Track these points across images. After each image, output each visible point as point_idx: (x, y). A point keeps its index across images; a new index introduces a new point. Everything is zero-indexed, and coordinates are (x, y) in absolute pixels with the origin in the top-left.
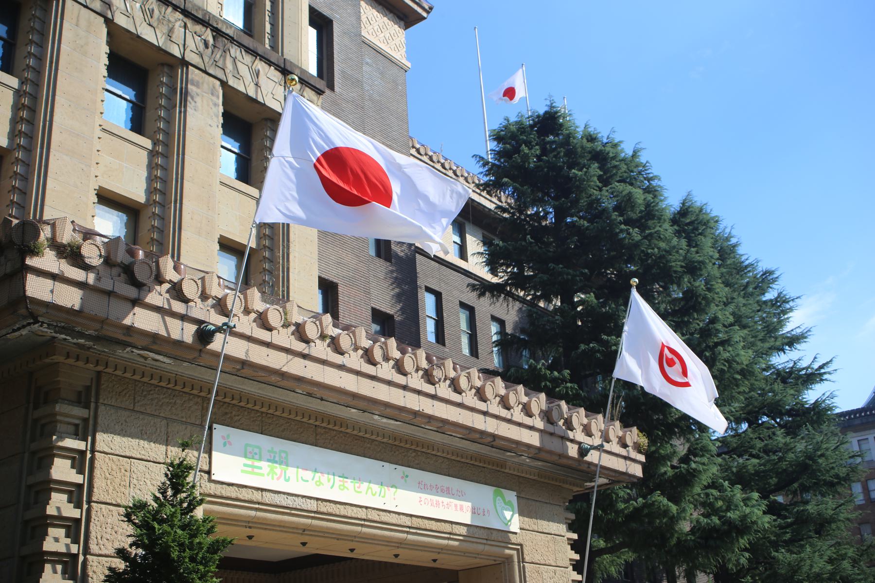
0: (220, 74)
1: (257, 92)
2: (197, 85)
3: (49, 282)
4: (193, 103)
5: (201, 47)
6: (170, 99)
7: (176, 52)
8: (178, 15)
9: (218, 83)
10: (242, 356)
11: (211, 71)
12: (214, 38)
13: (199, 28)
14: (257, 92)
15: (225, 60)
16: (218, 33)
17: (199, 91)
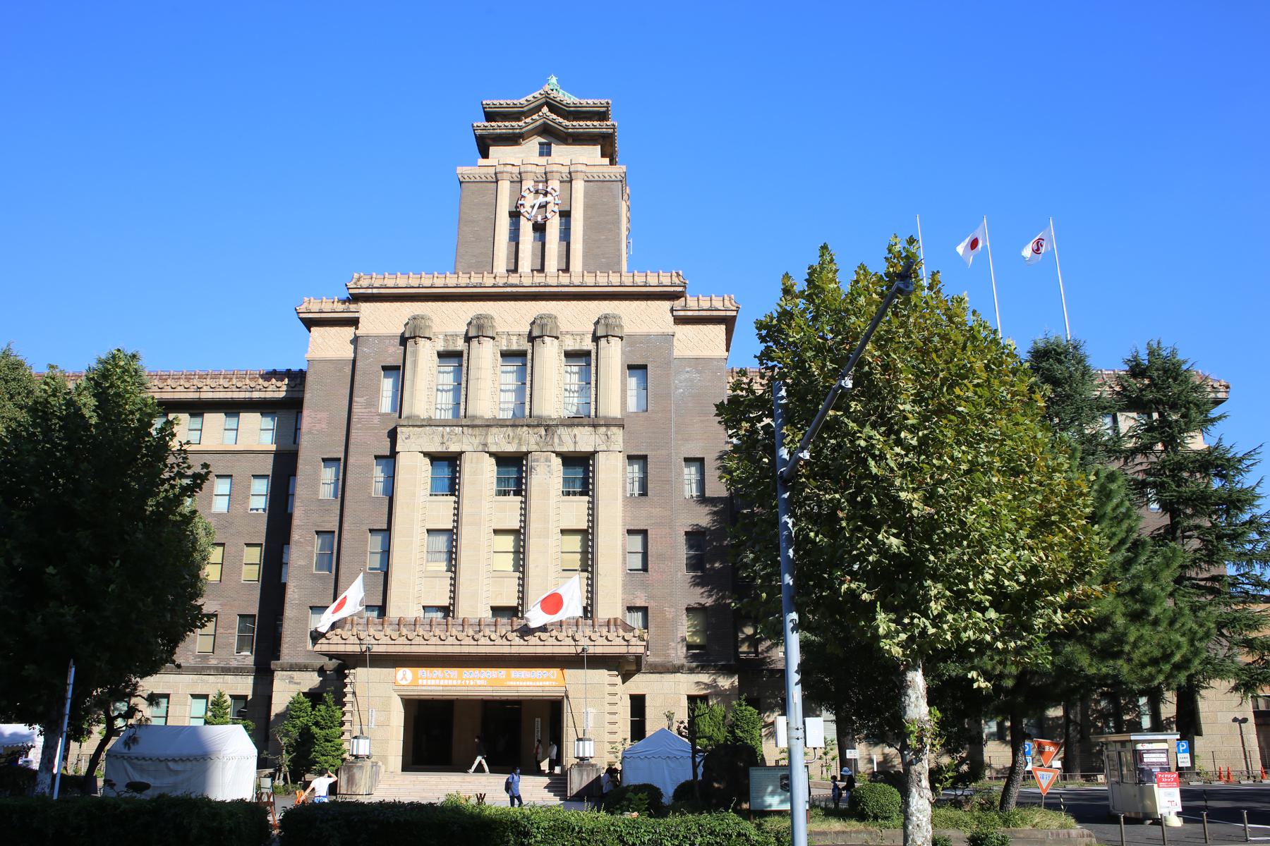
2: (537, 461)
5: (538, 438)
6: (526, 472)
7: (524, 449)
8: (525, 428)
13: (536, 430)
16: (548, 427)
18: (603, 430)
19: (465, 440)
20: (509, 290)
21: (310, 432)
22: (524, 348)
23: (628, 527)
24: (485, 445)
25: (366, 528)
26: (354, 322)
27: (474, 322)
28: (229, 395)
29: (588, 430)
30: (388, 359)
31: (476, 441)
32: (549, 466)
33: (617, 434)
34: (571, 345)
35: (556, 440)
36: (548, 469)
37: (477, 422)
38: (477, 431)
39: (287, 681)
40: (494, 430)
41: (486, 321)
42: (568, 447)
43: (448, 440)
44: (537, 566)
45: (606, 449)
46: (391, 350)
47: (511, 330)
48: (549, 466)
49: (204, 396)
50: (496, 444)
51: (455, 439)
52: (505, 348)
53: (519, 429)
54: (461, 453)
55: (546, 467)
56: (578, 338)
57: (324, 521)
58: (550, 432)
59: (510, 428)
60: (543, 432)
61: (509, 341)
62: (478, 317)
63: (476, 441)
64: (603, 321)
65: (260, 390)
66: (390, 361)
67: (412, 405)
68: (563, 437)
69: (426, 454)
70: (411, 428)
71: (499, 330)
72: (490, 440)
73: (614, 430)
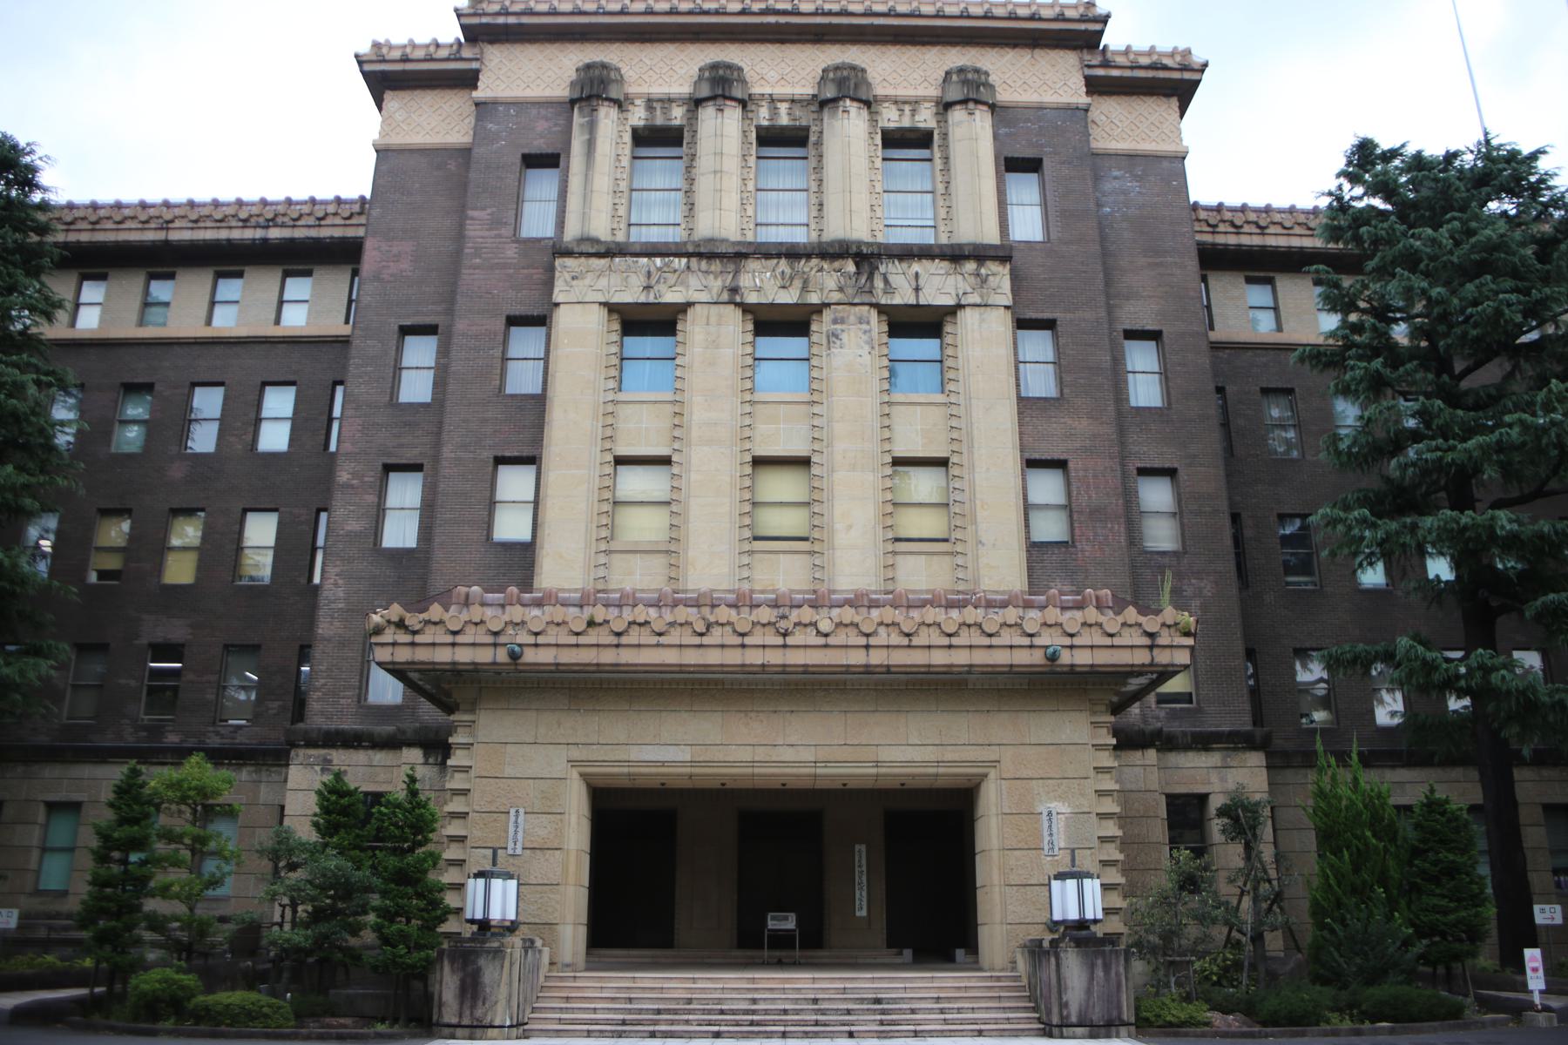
0: (866, 298)
1: (917, 297)
3: (389, 649)
4: (838, 342)
7: (814, 299)
9: (867, 308)
10: (551, 660)
11: (856, 301)
12: (857, 265)
13: (837, 264)
14: (917, 297)
15: (872, 281)
17: (844, 327)
18: (970, 266)
19: (694, 281)
20: (772, 19)
21: (377, 278)
22: (804, 123)
23: (1027, 455)
24: (734, 290)
25: (488, 455)
26: (468, 80)
27: (707, 74)
28: (223, 235)
29: (940, 266)
30: (536, 143)
31: (716, 284)
32: (865, 332)
33: (1000, 277)
34: (891, 118)
35: (879, 283)
36: (865, 337)
37: (722, 249)
38: (716, 266)
39: (318, 768)
40: (753, 264)
41: (728, 72)
42: (903, 296)
43: (658, 282)
44: (850, 527)
45: (978, 300)
46: (541, 126)
47: (778, 91)
48: (865, 332)
49: (175, 236)
50: (759, 290)
51: (672, 278)
52: (766, 123)
53: (803, 261)
54: (684, 308)
55: (860, 334)
56: (907, 108)
57: (401, 446)
58: (866, 267)
59: (783, 261)
60: (850, 267)
61: (774, 111)
62: (715, 67)
63: (716, 284)
64: (955, 77)
65: (283, 226)
66: (539, 145)
67: (585, 217)
68: (891, 278)
69: (612, 308)
70: (583, 260)
71: (756, 90)
72: (745, 281)
73: (993, 267)
